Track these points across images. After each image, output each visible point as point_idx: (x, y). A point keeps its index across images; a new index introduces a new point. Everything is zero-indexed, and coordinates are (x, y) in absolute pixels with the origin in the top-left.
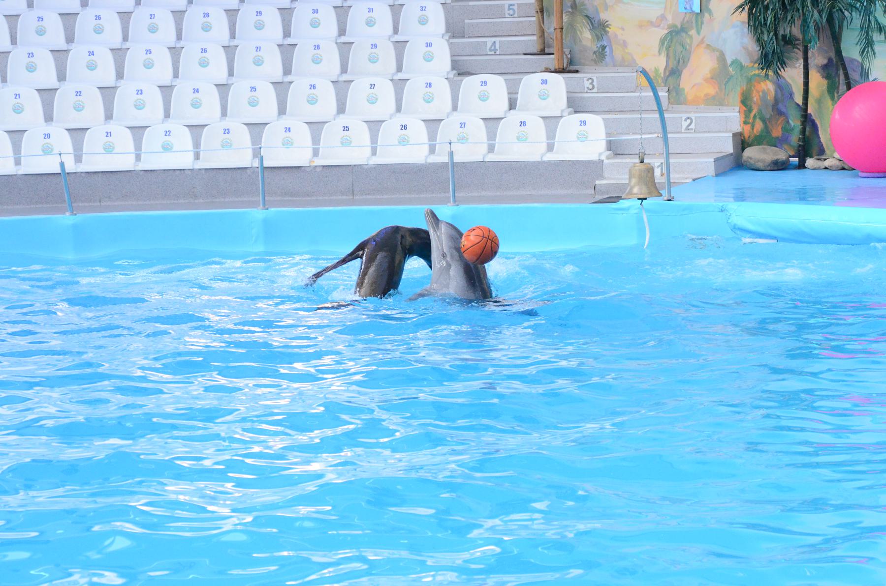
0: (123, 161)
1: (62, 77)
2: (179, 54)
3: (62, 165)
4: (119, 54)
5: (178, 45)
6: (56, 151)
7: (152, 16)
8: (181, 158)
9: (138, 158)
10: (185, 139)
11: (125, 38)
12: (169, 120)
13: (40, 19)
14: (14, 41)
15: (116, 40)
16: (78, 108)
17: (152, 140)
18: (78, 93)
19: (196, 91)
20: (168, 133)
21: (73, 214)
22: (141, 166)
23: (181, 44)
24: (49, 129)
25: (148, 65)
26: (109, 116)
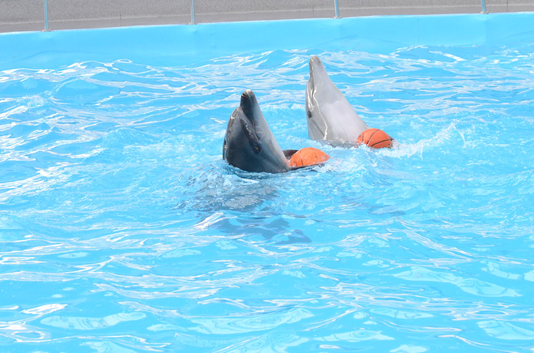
21: (486, 12)
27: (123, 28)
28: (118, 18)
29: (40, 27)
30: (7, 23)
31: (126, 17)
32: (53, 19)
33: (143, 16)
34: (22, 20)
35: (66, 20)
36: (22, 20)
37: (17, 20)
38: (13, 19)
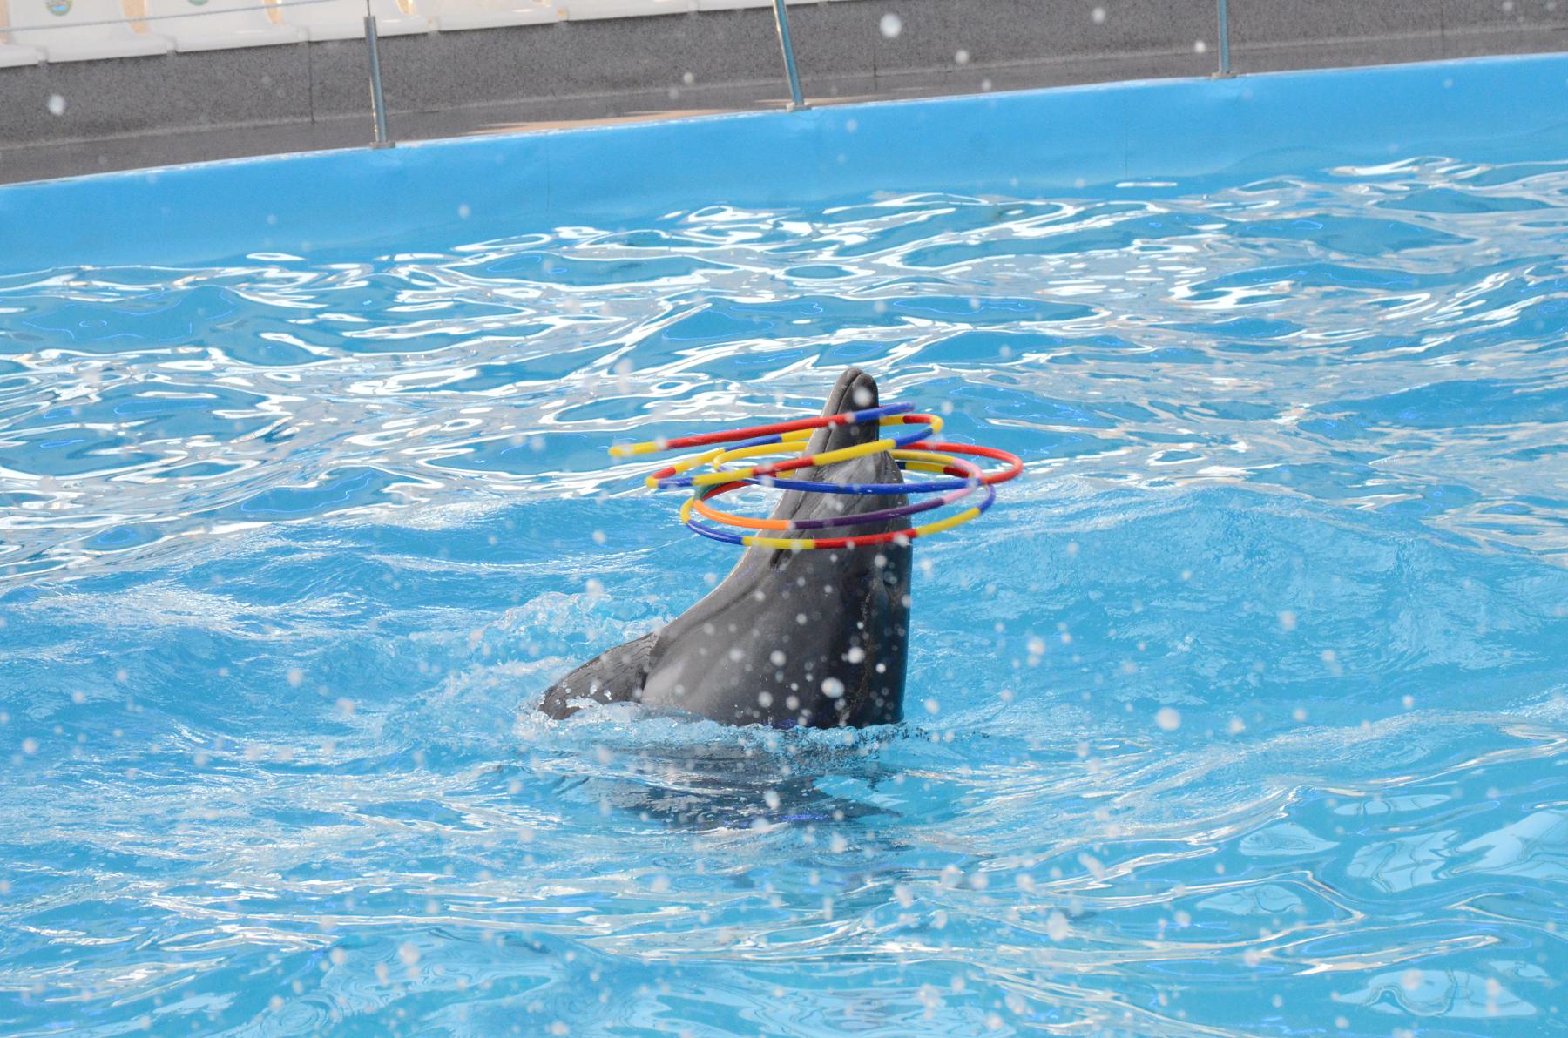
27: (1450, 62)
28: (1437, 33)
31: (1459, 31)
32: (1244, 41)
33: (1508, 28)
35: (1283, 44)
36: (1154, 45)
37: (1137, 46)
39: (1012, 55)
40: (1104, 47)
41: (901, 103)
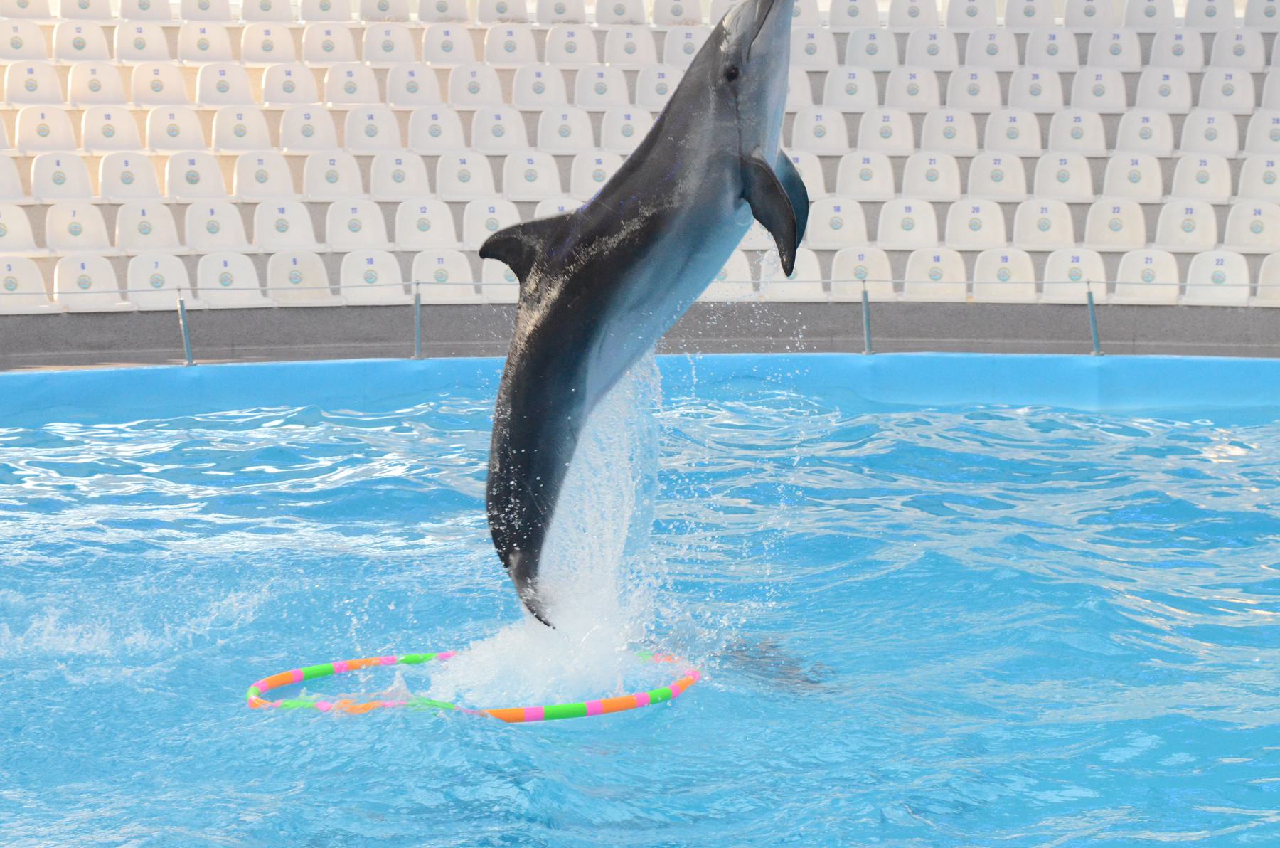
0: (1163, 293)
1: (1098, 189)
2: (1240, 168)
3: (1090, 295)
4: (1168, 164)
5: (1240, 156)
6: (1084, 279)
7: (1210, 120)
8: (1234, 294)
9: (1182, 290)
10: (1239, 271)
11: (1177, 146)
12: (1223, 246)
13: (1078, 119)
14: (1045, 145)
15: (1166, 148)
16: (1115, 227)
17: (1200, 270)
18: (1116, 210)
19: (1258, 212)
20: (1220, 262)
22: (1186, 300)
23: (1244, 154)
24: (1080, 251)
25: (1202, 179)
26: (1151, 239)
29: (408, 354)
30: (357, 344)
34: (381, 340)
38: (367, 339)
39: (306, 342)
40: (356, 340)
41: (245, 364)
